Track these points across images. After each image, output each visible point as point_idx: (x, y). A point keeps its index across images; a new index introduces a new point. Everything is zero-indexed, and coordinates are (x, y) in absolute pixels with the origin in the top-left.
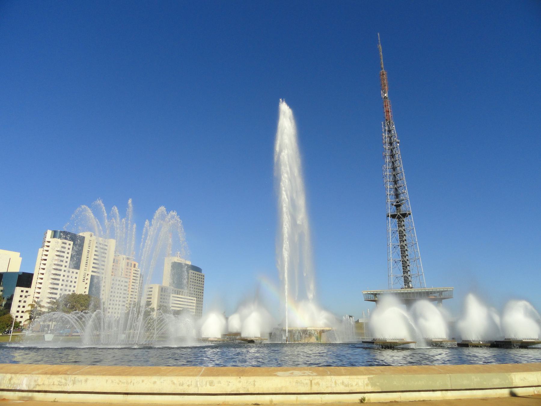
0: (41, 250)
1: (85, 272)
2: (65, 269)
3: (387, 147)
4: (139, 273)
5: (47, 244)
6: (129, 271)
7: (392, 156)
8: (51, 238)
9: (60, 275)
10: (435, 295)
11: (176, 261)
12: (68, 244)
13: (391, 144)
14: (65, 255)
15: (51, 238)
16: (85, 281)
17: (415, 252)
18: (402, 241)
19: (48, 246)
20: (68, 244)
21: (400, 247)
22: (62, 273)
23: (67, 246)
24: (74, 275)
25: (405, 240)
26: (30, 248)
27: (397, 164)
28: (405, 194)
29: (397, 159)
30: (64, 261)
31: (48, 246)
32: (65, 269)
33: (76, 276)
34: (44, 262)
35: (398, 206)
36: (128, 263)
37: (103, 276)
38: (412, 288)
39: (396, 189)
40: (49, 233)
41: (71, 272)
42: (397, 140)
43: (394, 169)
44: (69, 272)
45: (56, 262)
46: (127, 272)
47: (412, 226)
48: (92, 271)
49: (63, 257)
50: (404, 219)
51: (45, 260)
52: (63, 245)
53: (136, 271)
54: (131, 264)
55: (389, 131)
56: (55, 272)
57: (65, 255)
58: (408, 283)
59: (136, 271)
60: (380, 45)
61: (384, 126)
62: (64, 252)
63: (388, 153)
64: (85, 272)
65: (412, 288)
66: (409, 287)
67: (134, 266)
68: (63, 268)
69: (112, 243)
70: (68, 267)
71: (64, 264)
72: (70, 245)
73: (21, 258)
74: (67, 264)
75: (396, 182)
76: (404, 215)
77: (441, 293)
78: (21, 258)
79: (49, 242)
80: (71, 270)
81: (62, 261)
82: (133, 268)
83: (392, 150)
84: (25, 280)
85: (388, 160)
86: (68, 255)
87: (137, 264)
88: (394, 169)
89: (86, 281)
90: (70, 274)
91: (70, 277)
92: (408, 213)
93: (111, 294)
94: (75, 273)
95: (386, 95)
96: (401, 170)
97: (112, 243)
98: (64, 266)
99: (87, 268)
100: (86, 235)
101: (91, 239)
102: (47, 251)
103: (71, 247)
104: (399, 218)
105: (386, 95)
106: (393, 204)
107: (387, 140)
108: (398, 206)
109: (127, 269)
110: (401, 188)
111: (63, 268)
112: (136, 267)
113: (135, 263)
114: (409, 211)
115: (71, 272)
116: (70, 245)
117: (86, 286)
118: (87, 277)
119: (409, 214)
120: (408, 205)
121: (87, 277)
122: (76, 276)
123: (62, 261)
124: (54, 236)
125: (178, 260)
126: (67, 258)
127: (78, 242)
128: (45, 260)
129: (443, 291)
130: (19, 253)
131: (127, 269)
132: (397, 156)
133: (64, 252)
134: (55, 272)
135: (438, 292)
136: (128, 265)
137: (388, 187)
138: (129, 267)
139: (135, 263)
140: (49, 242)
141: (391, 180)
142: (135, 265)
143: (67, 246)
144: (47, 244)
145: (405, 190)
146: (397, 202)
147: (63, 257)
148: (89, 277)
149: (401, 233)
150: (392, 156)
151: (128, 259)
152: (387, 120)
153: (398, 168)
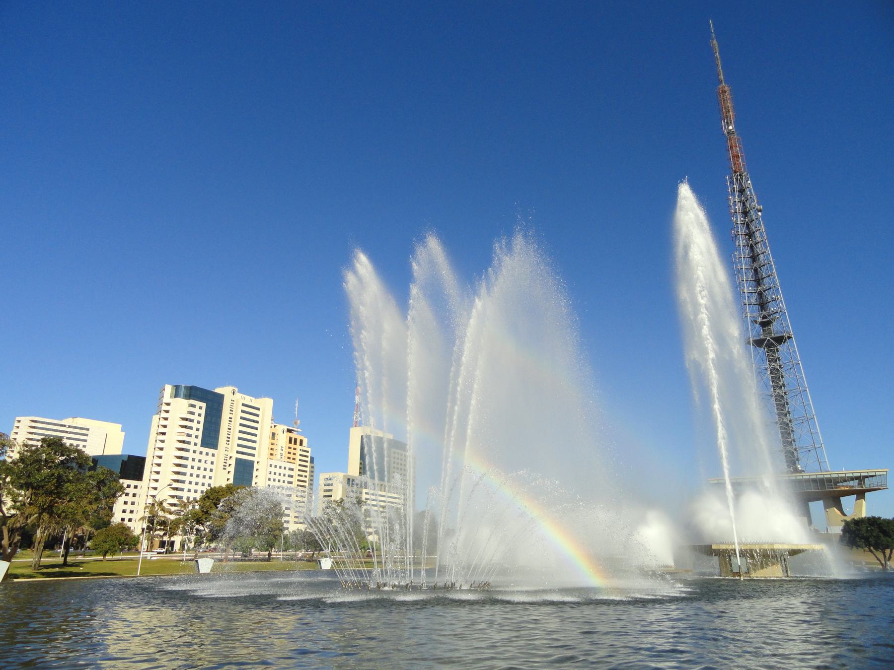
0: (155, 418)
1: (226, 453)
2: (195, 448)
3: (740, 219)
5: (165, 407)
6: (292, 451)
7: (750, 235)
8: (171, 397)
9: (186, 459)
10: (848, 483)
12: (198, 407)
13: (745, 213)
14: (194, 425)
15: (171, 397)
16: (227, 467)
17: (806, 402)
18: (777, 386)
19: (167, 412)
20: (198, 407)
21: (773, 398)
22: (190, 455)
23: (196, 410)
24: (210, 459)
25: (784, 385)
26: (137, 414)
27: (759, 249)
28: (779, 303)
29: (759, 239)
30: (193, 436)
31: (167, 412)
32: (195, 448)
33: (213, 459)
34: (162, 437)
35: (765, 324)
36: (291, 439)
38: (801, 471)
39: (760, 294)
40: (169, 389)
42: (757, 207)
43: (754, 258)
46: (289, 453)
47: (796, 360)
48: (238, 452)
49: (191, 428)
50: (780, 347)
51: (164, 434)
52: (192, 409)
54: (296, 440)
55: (742, 191)
57: (194, 425)
58: (795, 464)
60: (715, 41)
61: (732, 182)
62: (192, 421)
63: (742, 230)
64: (226, 453)
65: (801, 471)
66: (796, 470)
67: (301, 444)
68: (191, 447)
69: (266, 405)
70: (199, 444)
71: (192, 440)
73: (123, 434)
74: (199, 441)
75: (758, 281)
76: (780, 340)
77: (861, 479)
78: (123, 434)
79: (168, 404)
80: (205, 450)
81: (189, 435)
82: (298, 447)
83: (748, 226)
84: (133, 467)
85: (742, 242)
88: (754, 258)
89: (228, 469)
90: (203, 457)
91: (203, 461)
92: (786, 335)
94: (210, 455)
95: (731, 128)
96: (768, 259)
97: (266, 405)
98: (192, 444)
101: (233, 397)
102: (166, 419)
103: (203, 412)
104: (770, 345)
105: (731, 128)
106: (756, 322)
107: (739, 207)
108: (765, 324)
109: (290, 448)
110: (771, 291)
111: (191, 447)
113: (302, 438)
114: (788, 333)
115: (204, 453)
116: (201, 408)
118: (229, 462)
119: (789, 338)
120: (785, 320)
121: (229, 462)
122: (213, 459)
123: (189, 435)
124: (176, 395)
127: (214, 404)
128: (164, 434)
129: (867, 477)
130: (120, 426)
131: (290, 448)
132: (758, 234)
133: (192, 421)
135: (857, 478)
136: (290, 442)
137: (746, 291)
138: (292, 446)
139: (302, 438)
140: (168, 404)
141: (750, 278)
142: (301, 442)
143: (196, 410)
144: (165, 407)
145: (778, 294)
146: (765, 317)
147: (191, 428)
148: (233, 462)
149: (774, 371)
150: (750, 235)
151: (289, 431)
152: (735, 172)
153: (761, 256)
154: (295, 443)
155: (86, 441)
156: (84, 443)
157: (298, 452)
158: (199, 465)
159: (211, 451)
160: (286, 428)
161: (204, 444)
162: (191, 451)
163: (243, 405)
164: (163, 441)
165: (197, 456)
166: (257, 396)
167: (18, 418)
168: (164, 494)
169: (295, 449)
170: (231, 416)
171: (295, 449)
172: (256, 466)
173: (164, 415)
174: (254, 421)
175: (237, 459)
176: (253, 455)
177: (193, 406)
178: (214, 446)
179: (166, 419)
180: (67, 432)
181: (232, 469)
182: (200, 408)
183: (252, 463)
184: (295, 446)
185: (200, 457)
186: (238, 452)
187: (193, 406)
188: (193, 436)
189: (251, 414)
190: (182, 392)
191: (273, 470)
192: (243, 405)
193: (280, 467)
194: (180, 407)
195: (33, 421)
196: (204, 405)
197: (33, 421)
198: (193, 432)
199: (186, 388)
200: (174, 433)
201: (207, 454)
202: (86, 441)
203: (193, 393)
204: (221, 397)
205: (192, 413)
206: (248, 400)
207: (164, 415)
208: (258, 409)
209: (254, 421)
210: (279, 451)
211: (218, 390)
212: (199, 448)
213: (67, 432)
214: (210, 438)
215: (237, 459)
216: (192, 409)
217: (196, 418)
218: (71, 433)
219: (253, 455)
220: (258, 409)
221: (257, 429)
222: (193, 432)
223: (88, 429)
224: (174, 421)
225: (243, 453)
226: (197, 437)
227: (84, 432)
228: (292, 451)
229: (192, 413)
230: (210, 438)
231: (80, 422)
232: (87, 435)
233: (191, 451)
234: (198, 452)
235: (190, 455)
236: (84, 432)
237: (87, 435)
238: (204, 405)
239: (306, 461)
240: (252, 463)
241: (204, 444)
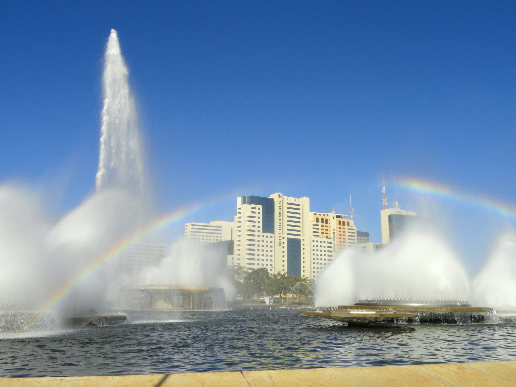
0: (236, 218)
1: (280, 235)
2: (259, 234)
4: (355, 231)
5: (239, 211)
9: (254, 241)
11: (394, 213)
12: (257, 208)
14: (256, 219)
19: (240, 213)
20: (257, 208)
22: (256, 238)
23: (256, 210)
24: (269, 239)
31: (240, 213)
32: (259, 234)
33: (272, 240)
34: (239, 229)
36: (340, 222)
37: (301, 238)
40: (239, 200)
41: (265, 236)
44: (263, 236)
45: (249, 228)
46: (340, 231)
48: (288, 234)
49: (254, 222)
51: (240, 227)
52: (254, 210)
53: (350, 229)
54: (344, 223)
56: (249, 238)
57: (256, 219)
59: (350, 229)
64: (280, 235)
67: (348, 225)
68: (256, 233)
69: (305, 202)
70: (261, 231)
71: (256, 229)
72: (259, 209)
74: (261, 229)
79: (240, 209)
80: (265, 234)
81: (254, 226)
82: (346, 227)
86: (259, 220)
87: (352, 222)
89: (283, 245)
90: (265, 239)
93: (313, 257)
97: (305, 202)
99: (282, 232)
100: (274, 196)
101: (281, 200)
102: (240, 217)
103: (261, 211)
111: (256, 233)
112: (351, 224)
113: (348, 220)
115: (265, 236)
116: (259, 209)
117: (284, 250)
118: (282, 241)
121: (282, 241)
122: (272, 240)
123: (254, 226)
124: (244, 202)
125: (396, 212)
127: (268, 207)
128: (240, 227)
131: (340, 228)
134: (249, 238)
136: (340, 224)
138: (342, 226)
139: (348, 220)
140: (240, 209)
143: (256, 210)
144: (239, 211)
147: (254, 222)
148: (285, 240)
151: (337, 217)
154: (344, 224)
155: (221, 234)
157: (347, 231)
158: (263, 244)
159: (270, 235)
160: (335, 215)
161: (264, 230)
162: (256, 236)
163: (288, 204)
164: (240, 231)
166: (299, 197)
167: (186, 224)
168: (244, 263)
169: (344, 228)
170: (280, 212)
171: (344, 228)
172: (302, 242)
173: (239, 215)
174: (297, 213)
175: (288, 239)
176: (300, 235)
177: (254, 208)
178: (272, 231)
179: (240, 217)
180: (210, 230)
181: (285, 245)
182: (259, 209)
183: (299, 240)
184: (344, 227)
186: (288, 234)
187: (254, 208)
189: (294, 208)
190: (247, 200)
191: (315, 244)
192: (288, 204)
193: (321, 242)
194: (246, 210)
195: (193, 225)
197: (193, 225)
198: (256, 224)
199: (249, 197)
200: (246, 226)
201: (267, 237)
202: (221, 234)
203: (253, 200)
204: (273, 200)
205: (254, 213)
206: (292, 200)
207: (239, 215)
208: (299, 205)
209: (297, 213)
210: (332, 231)
211: (271, 197)
212: (261, 234)
213: (210, 230)
214: (268, 225)
215: (288, 239)
216: (254, 210)
217: (256, 215)
218: (207, 229)
219: (300, 235)
220: (299, 205)
221: (299, 218)
222: (256, 224)
223: (221, 227)
224: (245, 219)
225: (292, 234)
226: (259, 227)
227: (219, 229)
228: (342, 230)
229: (254, 213)
230: (268, 225)
231: (217, 223)
233: (256, 236)
234: (261, 236)
235: (256, 238)
236: (219, 229)
239: (354, 236)
240: (299, 240)
241: (264, 230)
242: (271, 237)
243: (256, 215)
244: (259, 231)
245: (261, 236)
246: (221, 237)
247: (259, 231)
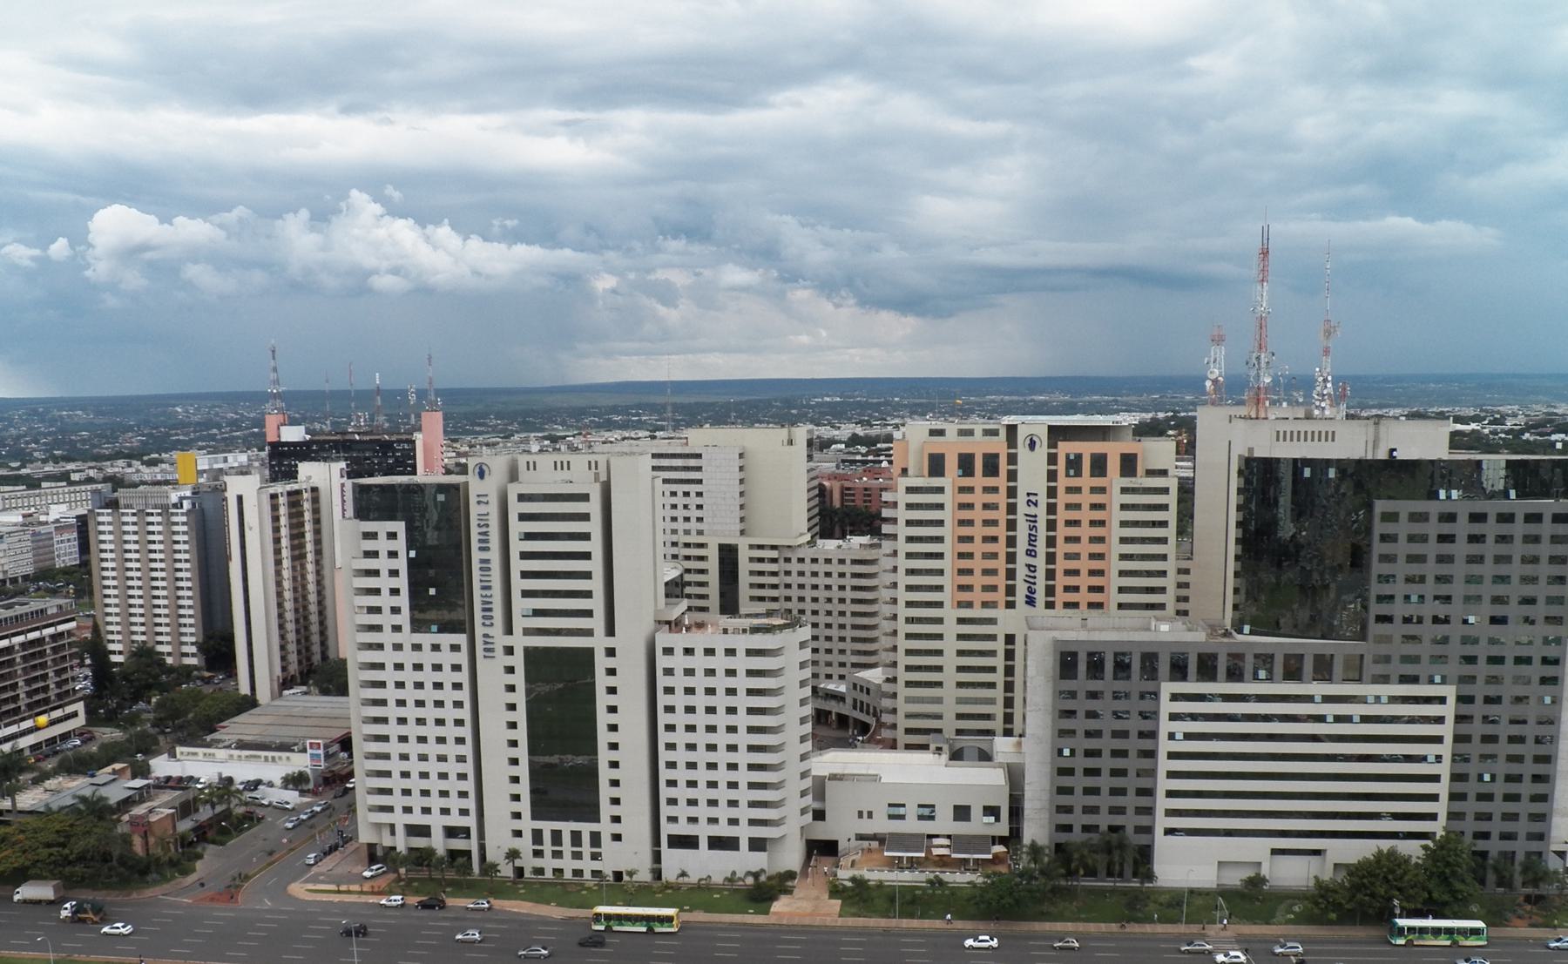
2: (398, 638)
20: (382, 536)
23: (383, 545)
32: (398, 638)
52: (370, 545)
70: (407, 627)
71: (386, 619)
72: (392, 536)
74: (404, 619)
81: (378, 610)
86: (394, 583)
103: (400, 544)
116: (392, 536)
123: (378, 610)
126: (395, 592)
143: (383, 545)
155: (700, 482)
156: (698, 488)
165: (408, 657)
185: (416, 657)
188: (386, 610)
196: (399, 527)
198: (384, 600)
202: (700, 482)
205: (373, 554)
212: (407, 637)
216: (370, 545)
223: (699, 456)
226: (396, 610)
227: (692, 462)
229: (373, 554)
232: (699, 469)
236: (692, 462)
237: (699, 469)
238: (399, 527)
242: (455, 648)
243: (383, 564)
244: (397, 628)
245: (407, 647)
246: (699, 494)
247: (397, 628)
